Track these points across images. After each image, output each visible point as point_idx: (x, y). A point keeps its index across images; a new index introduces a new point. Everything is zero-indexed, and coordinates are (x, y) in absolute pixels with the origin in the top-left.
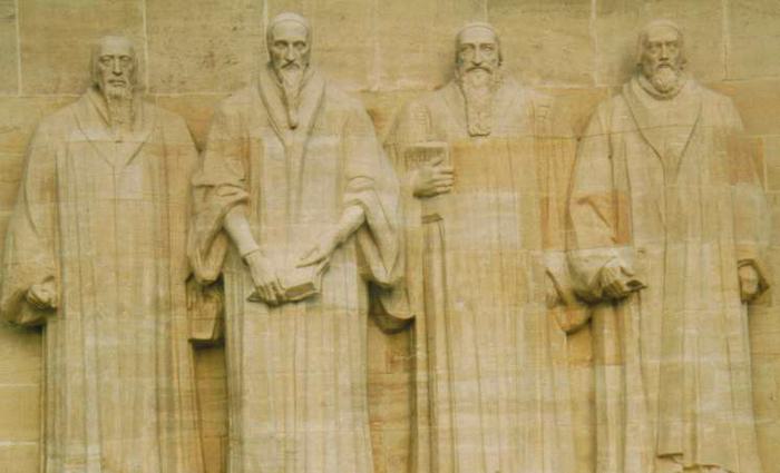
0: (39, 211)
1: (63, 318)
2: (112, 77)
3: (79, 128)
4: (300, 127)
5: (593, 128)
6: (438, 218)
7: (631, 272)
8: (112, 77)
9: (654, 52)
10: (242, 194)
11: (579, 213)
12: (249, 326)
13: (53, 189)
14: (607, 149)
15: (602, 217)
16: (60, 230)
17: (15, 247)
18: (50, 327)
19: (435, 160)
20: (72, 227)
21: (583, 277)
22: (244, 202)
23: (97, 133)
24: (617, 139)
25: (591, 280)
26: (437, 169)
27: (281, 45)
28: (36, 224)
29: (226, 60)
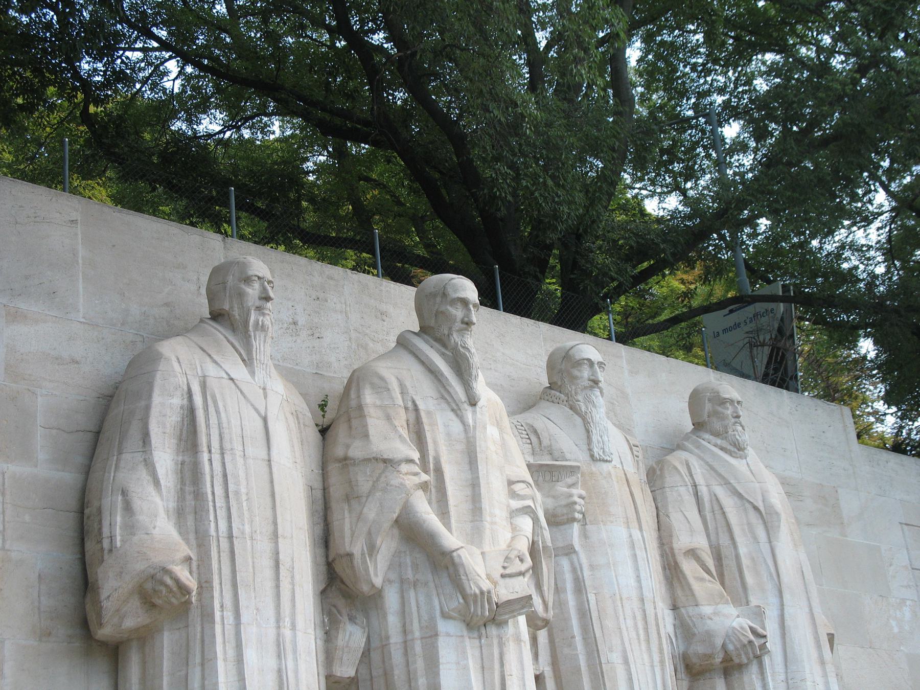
0: (165, 458)
1: (208, 616)
2: (258, 303)
3: (215, 362)
4: (480, 404)
5: (670, 479)
6: (570, 551)
7: (765, 633)
8: (258, 303)
9: (728, 409)
10: (425, 477)
11: (689, 567)
12: (447, 653)
13: (189, 437)
14: (693, 500)
15: (708, 572)
16: (198, 495)
17: (128, 508)
18: (167, 642)
19: (570, 480)
20: (219, 490)
21: (709, 636)
22: (424, 486)
23: (239, 372)
24: (703, 490)
25: (719, 642)
26: (575, 491)
27: (459, 305)
28: (162, 482)
29: (309, 332)
